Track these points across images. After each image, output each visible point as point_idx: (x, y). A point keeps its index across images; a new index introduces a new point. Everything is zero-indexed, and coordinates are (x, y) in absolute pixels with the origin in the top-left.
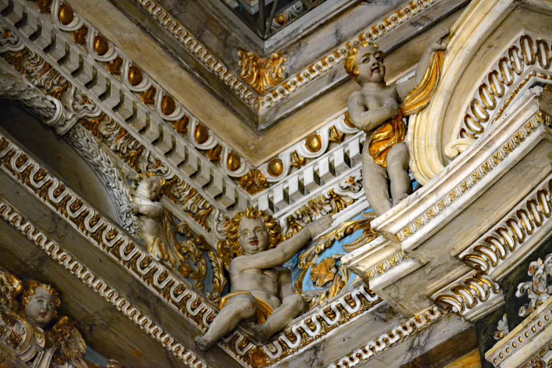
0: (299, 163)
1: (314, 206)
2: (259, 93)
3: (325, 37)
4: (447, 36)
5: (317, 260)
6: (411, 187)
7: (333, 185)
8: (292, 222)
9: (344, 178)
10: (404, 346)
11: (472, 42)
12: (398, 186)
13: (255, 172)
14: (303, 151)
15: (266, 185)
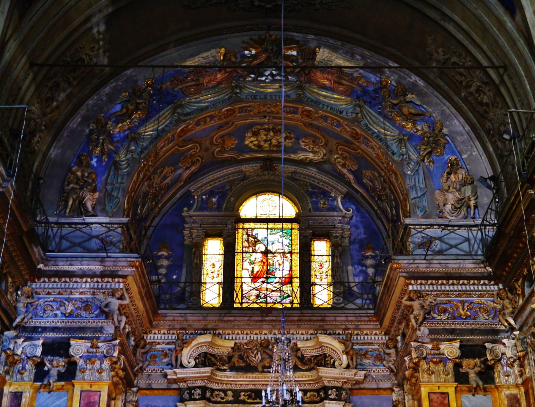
0: (155, 334)
1: (154, 342)
2: (155, 320)
3: (171, 318)
4: (196, 338)
5: (152, 353)
6: (182, 366)
7: (159, 341)
8: (149, 343)
9: (162, 341)
10: (166, 384)
11: (200, 341)
12: (179, 363)
13: (146, 331)
14: (157, 332)
15: (147, 334)
